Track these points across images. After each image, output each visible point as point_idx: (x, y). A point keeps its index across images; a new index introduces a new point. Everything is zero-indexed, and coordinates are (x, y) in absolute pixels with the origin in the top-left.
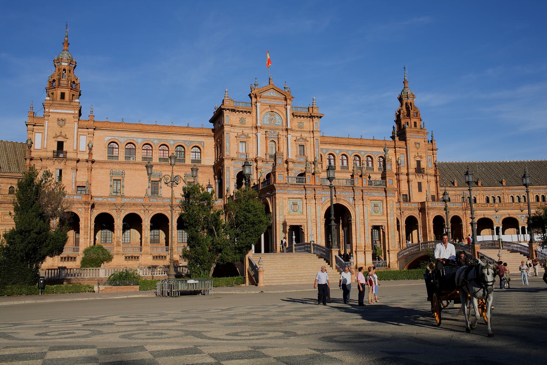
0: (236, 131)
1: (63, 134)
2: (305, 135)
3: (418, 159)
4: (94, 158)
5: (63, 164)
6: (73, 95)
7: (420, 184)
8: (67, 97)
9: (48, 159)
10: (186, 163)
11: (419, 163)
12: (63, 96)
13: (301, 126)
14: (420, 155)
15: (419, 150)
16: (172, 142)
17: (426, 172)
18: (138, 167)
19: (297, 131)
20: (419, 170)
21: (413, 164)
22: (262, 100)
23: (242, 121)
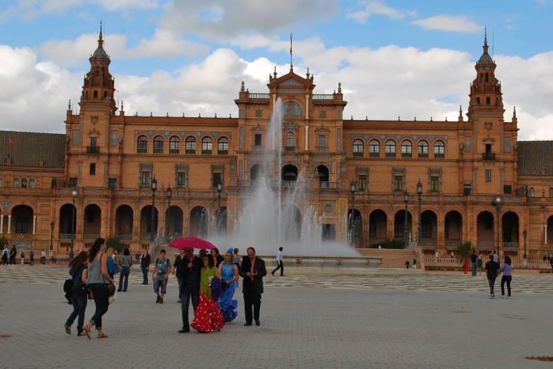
0: (252, 124)
1: (96, 130)
2: (326, 125)
3: (488, 142)
4: (126, 151)
5: (96, 158)
6: (106, 93)
7: (488, 172)
8: (99, 95)
9: (83, 154)
10: (213, 154)
11: (488, 147)
12: (96, 93)
13: (323, 115)
14: (491, 137)
15: (491, 131)
16: (199, 134)
17: (497, 157)
18: (166, 159)
19: (317, 120)
20: (489, 156)
21: (481, 149)
22: (280, 91)
23: (259, 113)
